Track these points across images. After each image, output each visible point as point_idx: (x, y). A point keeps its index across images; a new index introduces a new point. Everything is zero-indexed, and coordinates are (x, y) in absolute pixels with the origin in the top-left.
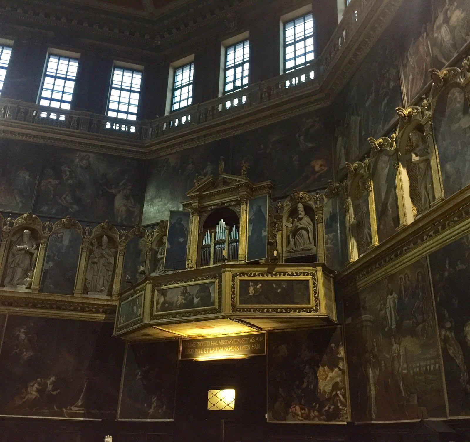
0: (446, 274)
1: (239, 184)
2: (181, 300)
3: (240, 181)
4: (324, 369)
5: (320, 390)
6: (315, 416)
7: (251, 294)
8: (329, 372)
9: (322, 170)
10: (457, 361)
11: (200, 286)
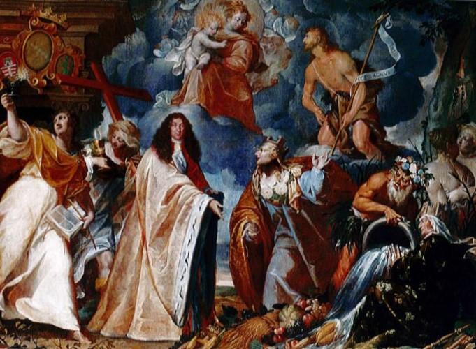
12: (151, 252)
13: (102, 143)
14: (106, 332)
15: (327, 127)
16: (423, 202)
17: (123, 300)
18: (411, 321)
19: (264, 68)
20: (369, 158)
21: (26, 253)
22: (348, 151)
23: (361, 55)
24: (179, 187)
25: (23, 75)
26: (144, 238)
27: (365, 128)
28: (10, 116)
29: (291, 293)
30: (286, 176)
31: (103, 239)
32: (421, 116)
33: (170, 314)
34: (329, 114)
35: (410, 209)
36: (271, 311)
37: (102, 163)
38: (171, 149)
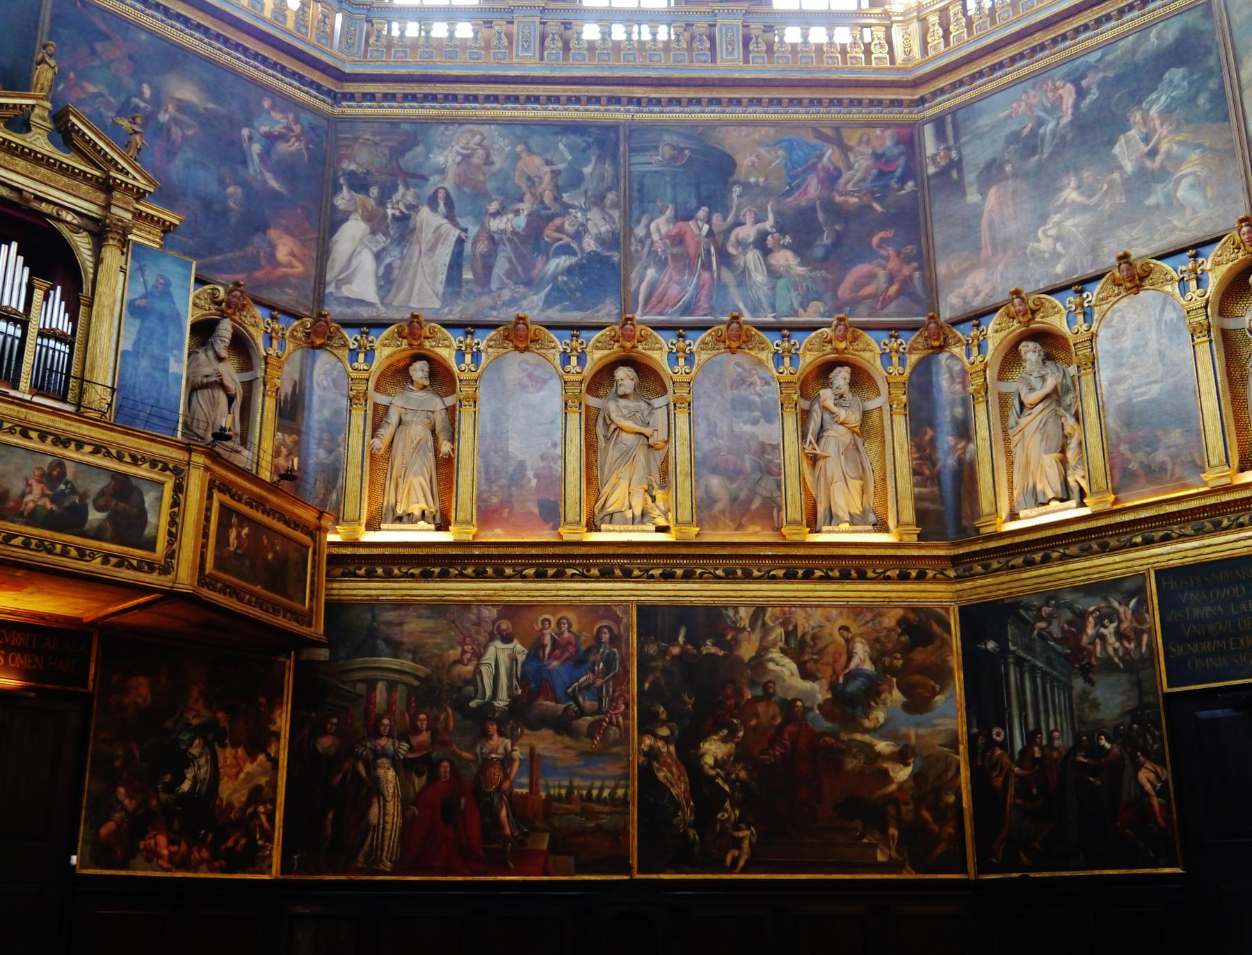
0: (676, 650)
1: (122, 181)
2: (36, 497)
3: (127, 173)
4: (237, 752)
5: (221, 800)
6: (203, 861)
7: (232, 549)
8: (245, 762)
9: (290, 266)
10: (674, 792)
11: (113, 477)
12: (424, 260)
13: (397, 202)
14: (395, 304)
17: (407, 285)
19: (492, 163)
21: (349, 261)
23: (549, 157)
25: (353, 167)
29: (507, 281)
30: (505, 219)
31: (396, 253)
32: (583, 187)
34: (530, 187)
35: (578, 236)
37: (397, 213)
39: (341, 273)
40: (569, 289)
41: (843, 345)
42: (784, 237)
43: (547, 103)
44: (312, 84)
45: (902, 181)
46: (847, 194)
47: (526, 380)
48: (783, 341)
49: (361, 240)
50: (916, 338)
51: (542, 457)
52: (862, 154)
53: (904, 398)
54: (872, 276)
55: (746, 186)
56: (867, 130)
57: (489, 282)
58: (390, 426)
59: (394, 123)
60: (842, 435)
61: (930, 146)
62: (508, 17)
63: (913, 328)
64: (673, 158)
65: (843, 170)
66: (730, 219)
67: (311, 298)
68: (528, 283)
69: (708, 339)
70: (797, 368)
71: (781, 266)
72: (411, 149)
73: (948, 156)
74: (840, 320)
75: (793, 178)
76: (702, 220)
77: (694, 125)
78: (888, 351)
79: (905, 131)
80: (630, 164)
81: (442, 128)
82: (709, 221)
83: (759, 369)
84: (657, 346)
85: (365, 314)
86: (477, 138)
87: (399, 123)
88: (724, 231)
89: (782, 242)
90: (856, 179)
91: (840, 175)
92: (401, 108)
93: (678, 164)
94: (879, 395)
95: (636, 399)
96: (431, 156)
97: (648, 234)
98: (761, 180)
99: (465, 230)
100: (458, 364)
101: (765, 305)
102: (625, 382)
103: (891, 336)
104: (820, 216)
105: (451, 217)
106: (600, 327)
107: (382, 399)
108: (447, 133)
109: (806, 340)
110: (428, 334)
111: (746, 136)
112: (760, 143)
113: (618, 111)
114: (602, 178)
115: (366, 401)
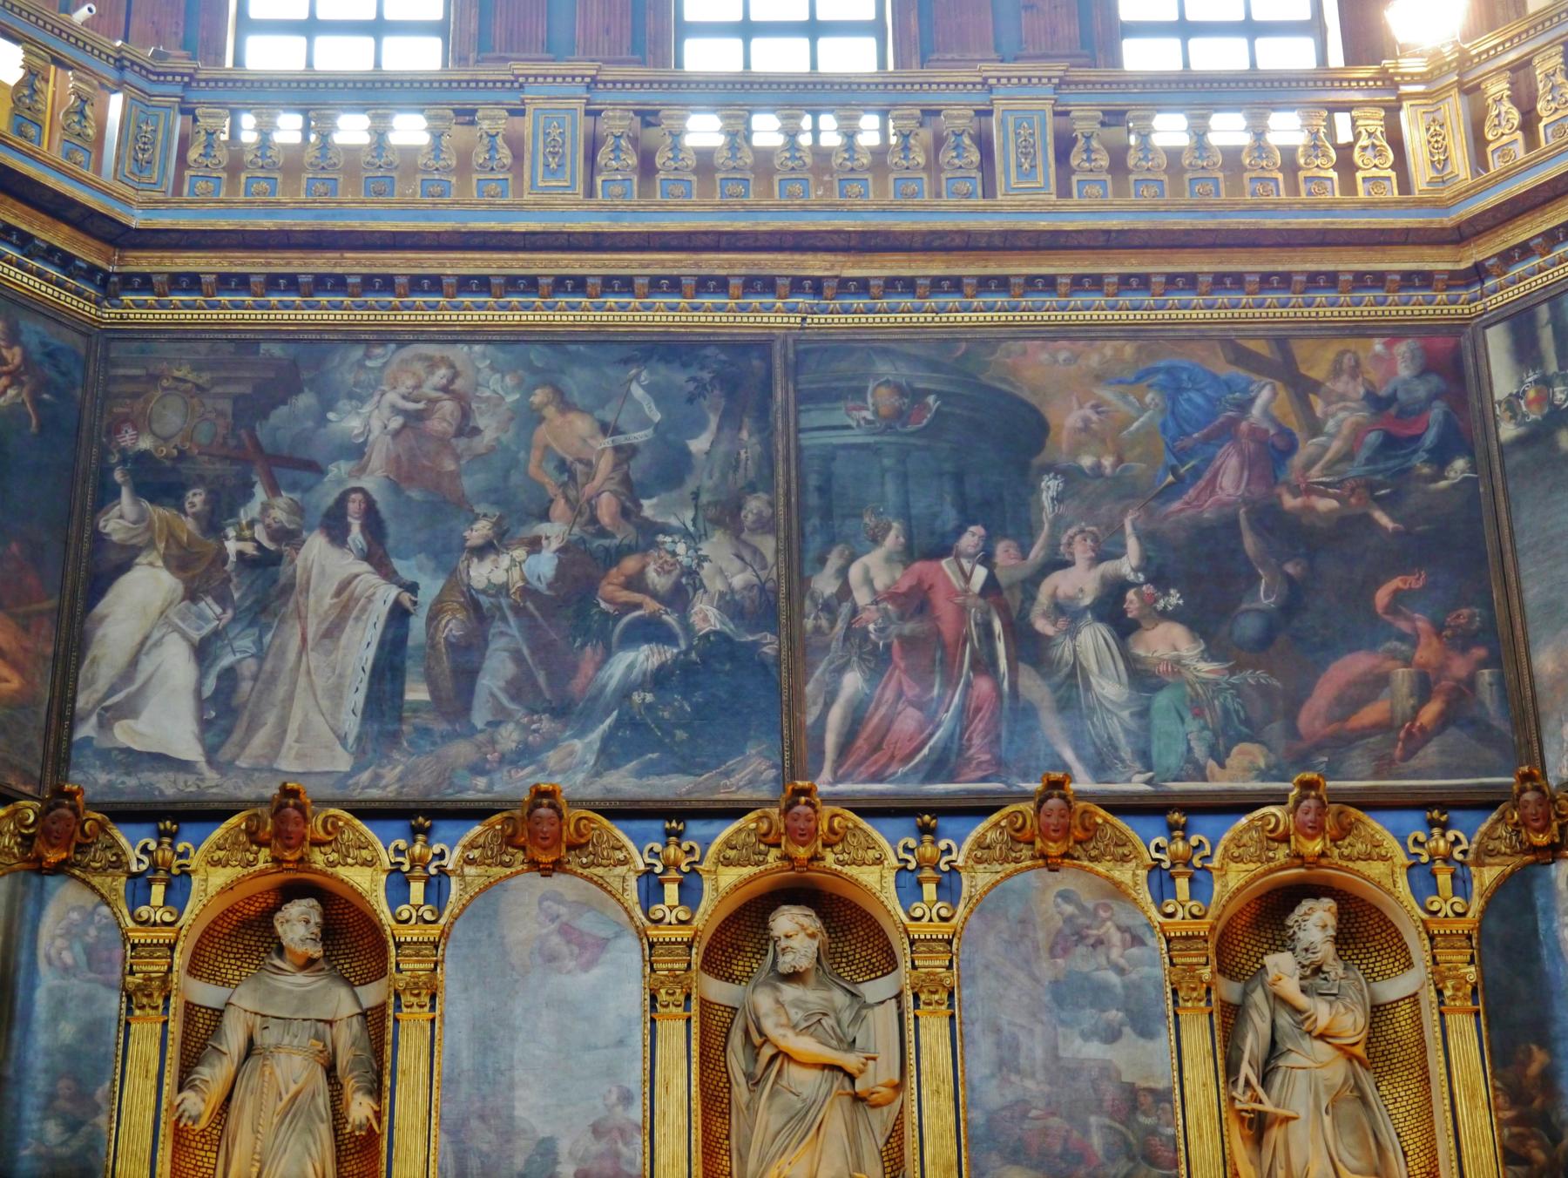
12: (314, 659)
13: (251, 525)
14: (242, 763)
15: (562, 502)
16: (696, 590)
17: (271, 719)
18: (682, 742)
19: (476, 431)
20: (620, 536)
21: (134, 663)
22: (591, 529)
23: (609, 417)
24: (357, 576)
25: (145, 443)
26: (304, 639)
27: (614, 501)
28: (125, 494)
29: (512, 706)
30: (505, 561)
31: (246, 643)
32: (690, 485)
33: (338, 737)
34: (564, 485)
35: (679, 597)
36: (482, 731)
37: (249, 548)
38: (346, 529)
39: (112, 690)
40: (659, 722)
41: (1316, 846)
42: (1166, 594)
43: (603, 294)
44: (51, 253)
45: (1441, 457)
46: (1310, 490)
47: (556, 941)
48: (1172, 839)
49: (162, 613)
50: (1493, 827)
51: (597, 1131)
52: (1343, 397)
53: (1471, 973)
54: (1378, 683)
55: (1071, 475)
56: (1351, 344)
57: (467, 709)
58: (225, 1060)
59: (245, 342)
60: (1323, 1066)
61: (1503, 378)
62: (512, 99)
63: (1483, 803)
64: (900, 415)
65: (1299, 435)
66: (1037, 553)
67: (39, 751)
68: (562, 711)
69: (992, 836)
70: (1207, 905)
71: (1161, 660)
72: (284, 402)
73: (1545, 398)
74: (1307, 785)
75: (1182, 455)
76: (970, 556)
77: (948, 339)
78: (1425, 859)
79: (1441, 343)
80: (799, 431)
81: (358, 352)
82: (987, 559)
83: (1115, 906)
84: (872, 854)
85: (168, 786)
86: (441, 374)
87: (257, 342)
88: (1023, 582)
89: (1161, 604)
90: (1328, 456)
91: (1292, 448)
92: (261, 306)
93: (911, 428)
94: (1409, 965)
95: (821, 984)
96: (331, 416)
97: (845, 592)
98: (1107, 462)
99: (412, 588)
100: (393, 906)
101: (1126, 752)
102: (794, 943)
103: (1432, 824)
104: (1250, 543)
105: (377, 557)
106: (732, 812)
107: (206, 994)
108: (369, 363)
109: (1227, 836)
110: (321, 834)
111: (1067, 361)
112: (1100, 378)
113: (769, 308)
114: (734, 464)
115: (167, 999)
